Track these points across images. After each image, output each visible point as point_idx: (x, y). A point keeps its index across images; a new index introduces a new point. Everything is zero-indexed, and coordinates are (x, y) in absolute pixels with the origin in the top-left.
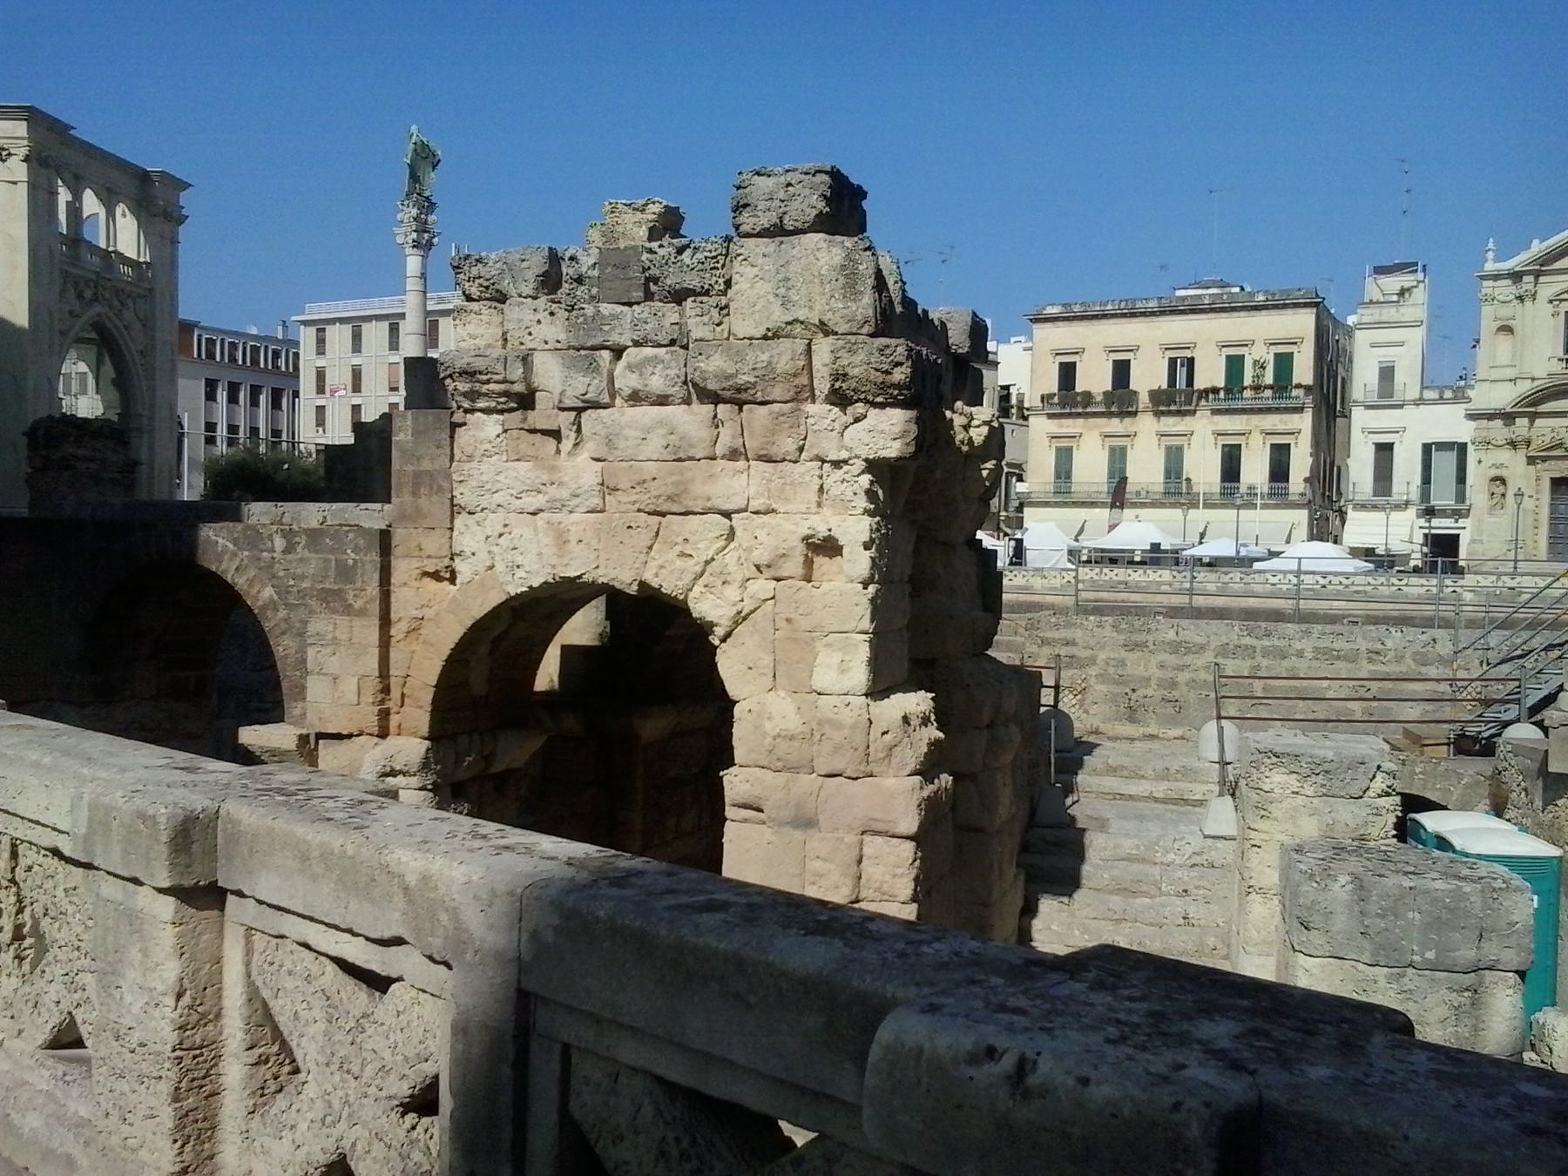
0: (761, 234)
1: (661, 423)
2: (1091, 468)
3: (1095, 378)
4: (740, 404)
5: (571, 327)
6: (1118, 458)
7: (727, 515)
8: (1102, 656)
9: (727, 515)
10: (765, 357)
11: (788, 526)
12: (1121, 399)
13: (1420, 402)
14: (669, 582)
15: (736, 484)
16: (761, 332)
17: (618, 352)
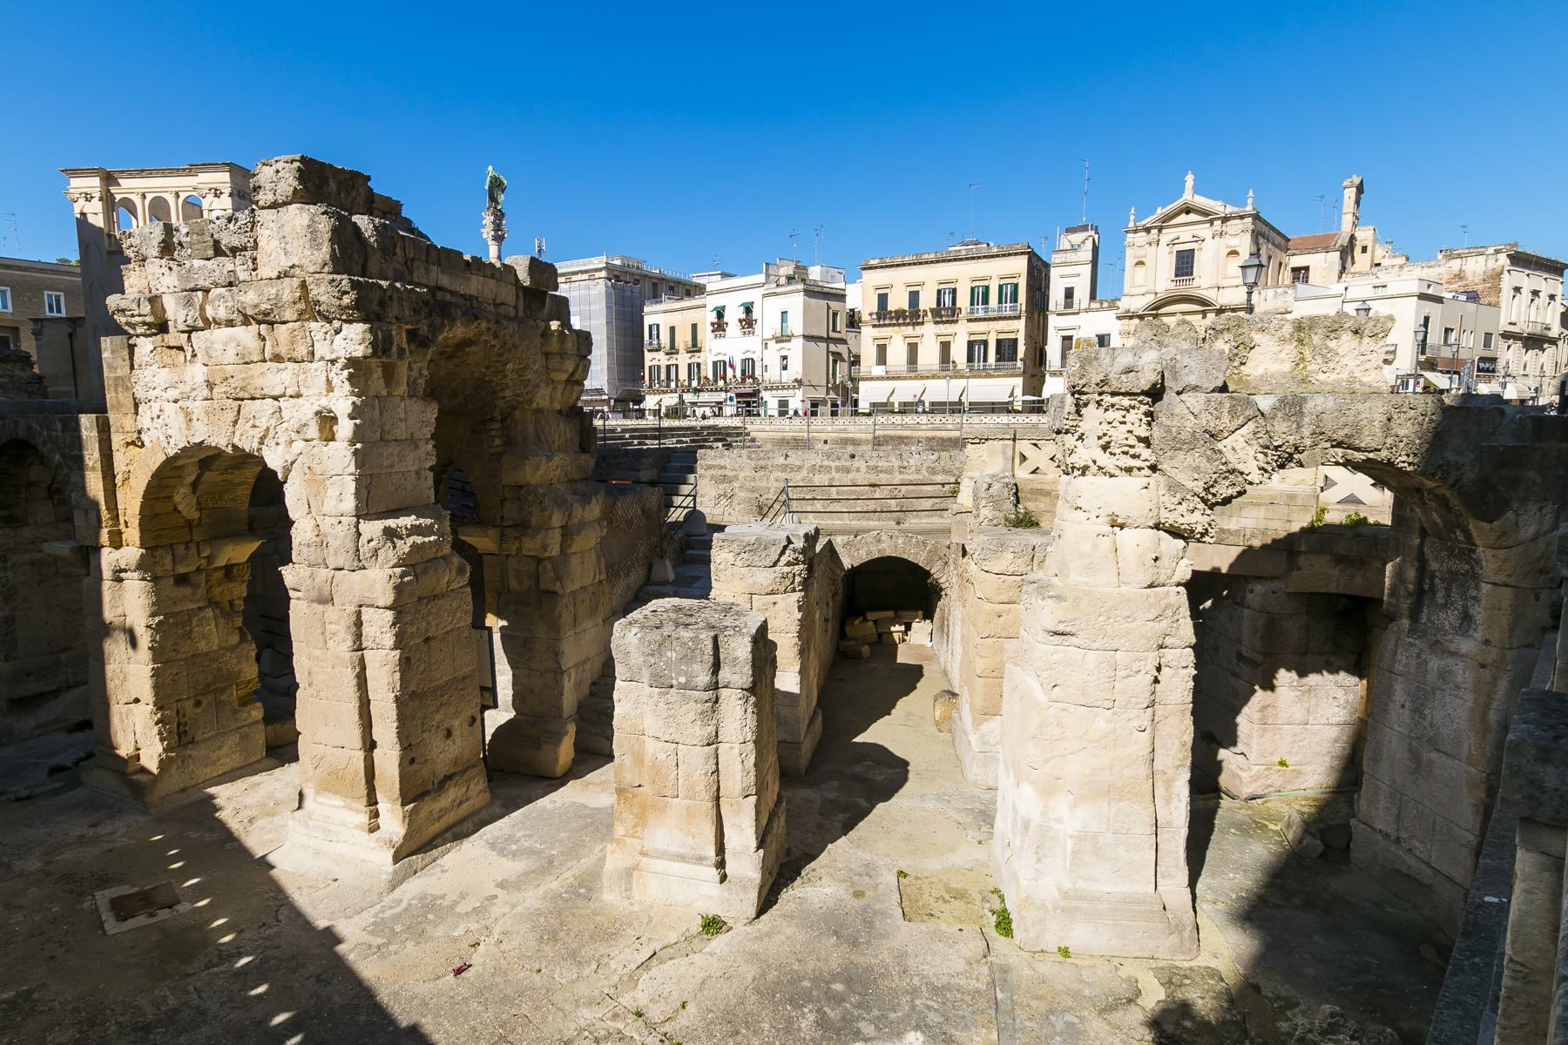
0: (270, 207)
1: (232, 339)
2: (897, 355)
3: (899, 301)
4: (272, 324)
5: (180, 277)
6: (913, 349)
7: (276, 398)
8: (742, 475)
9: (276, 398)
10: (273, 291)
11: (308, 404)
12: (912, 316)
13: (1087, 310)
14: (248, 444)
15: (277, 378)
16: (274, 275)
17: (207, 291)
